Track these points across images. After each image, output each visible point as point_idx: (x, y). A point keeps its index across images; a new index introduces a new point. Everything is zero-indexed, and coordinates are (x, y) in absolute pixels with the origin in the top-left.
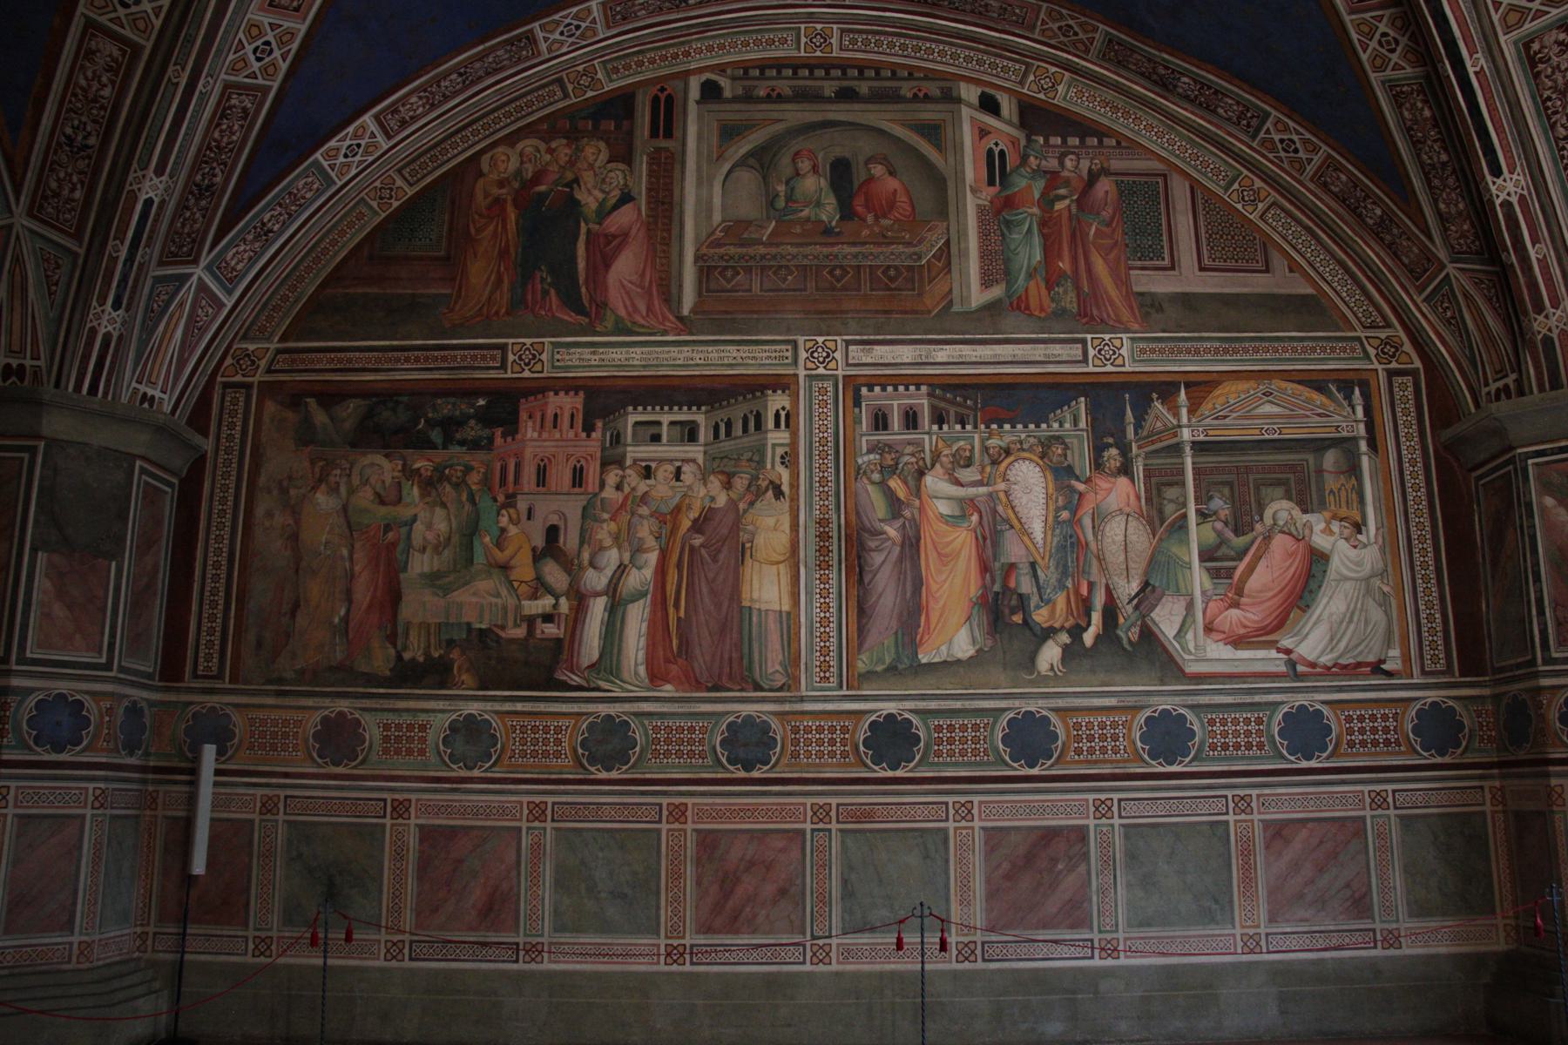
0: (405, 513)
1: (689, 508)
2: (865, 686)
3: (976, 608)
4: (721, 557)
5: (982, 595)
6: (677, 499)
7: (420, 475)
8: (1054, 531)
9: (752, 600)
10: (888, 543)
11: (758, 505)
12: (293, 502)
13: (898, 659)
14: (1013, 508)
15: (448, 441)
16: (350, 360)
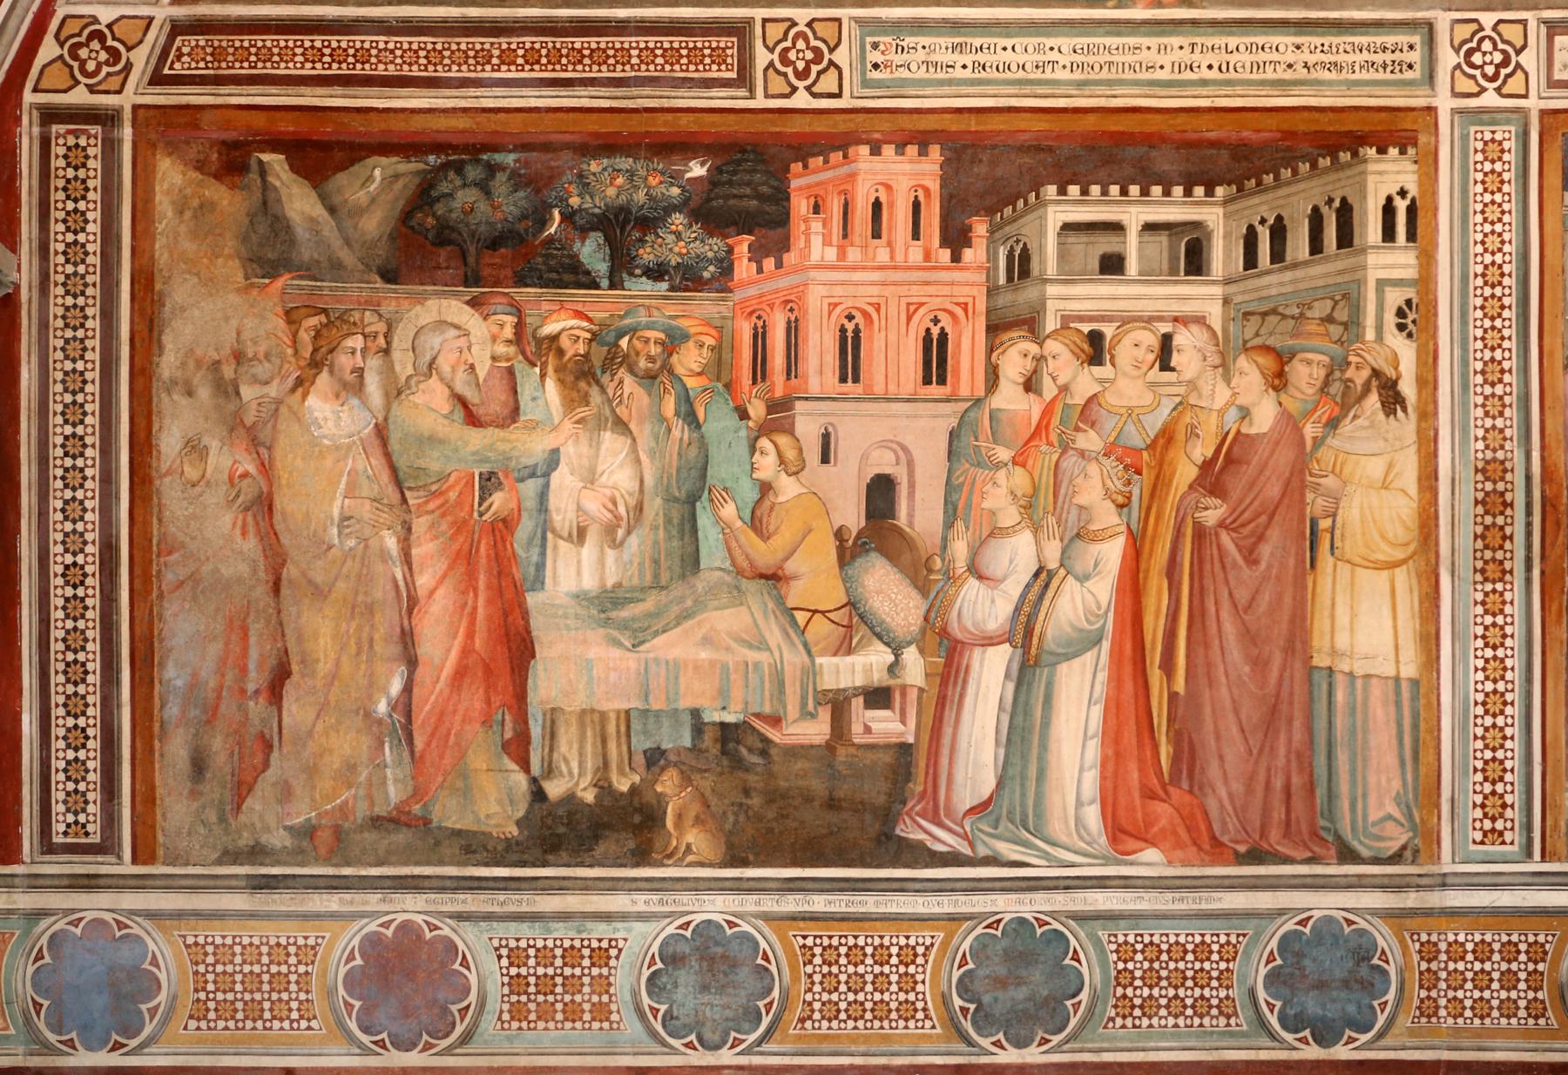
0: (534, 447)
1: (1192, 433)
4: (1265, 550)
6: (1164, 412)
7: (561, 352)
9: (1334, 652)
11: (1346, 427)
12: (249, 419)
15: (622, 264)
16: (362, 56)
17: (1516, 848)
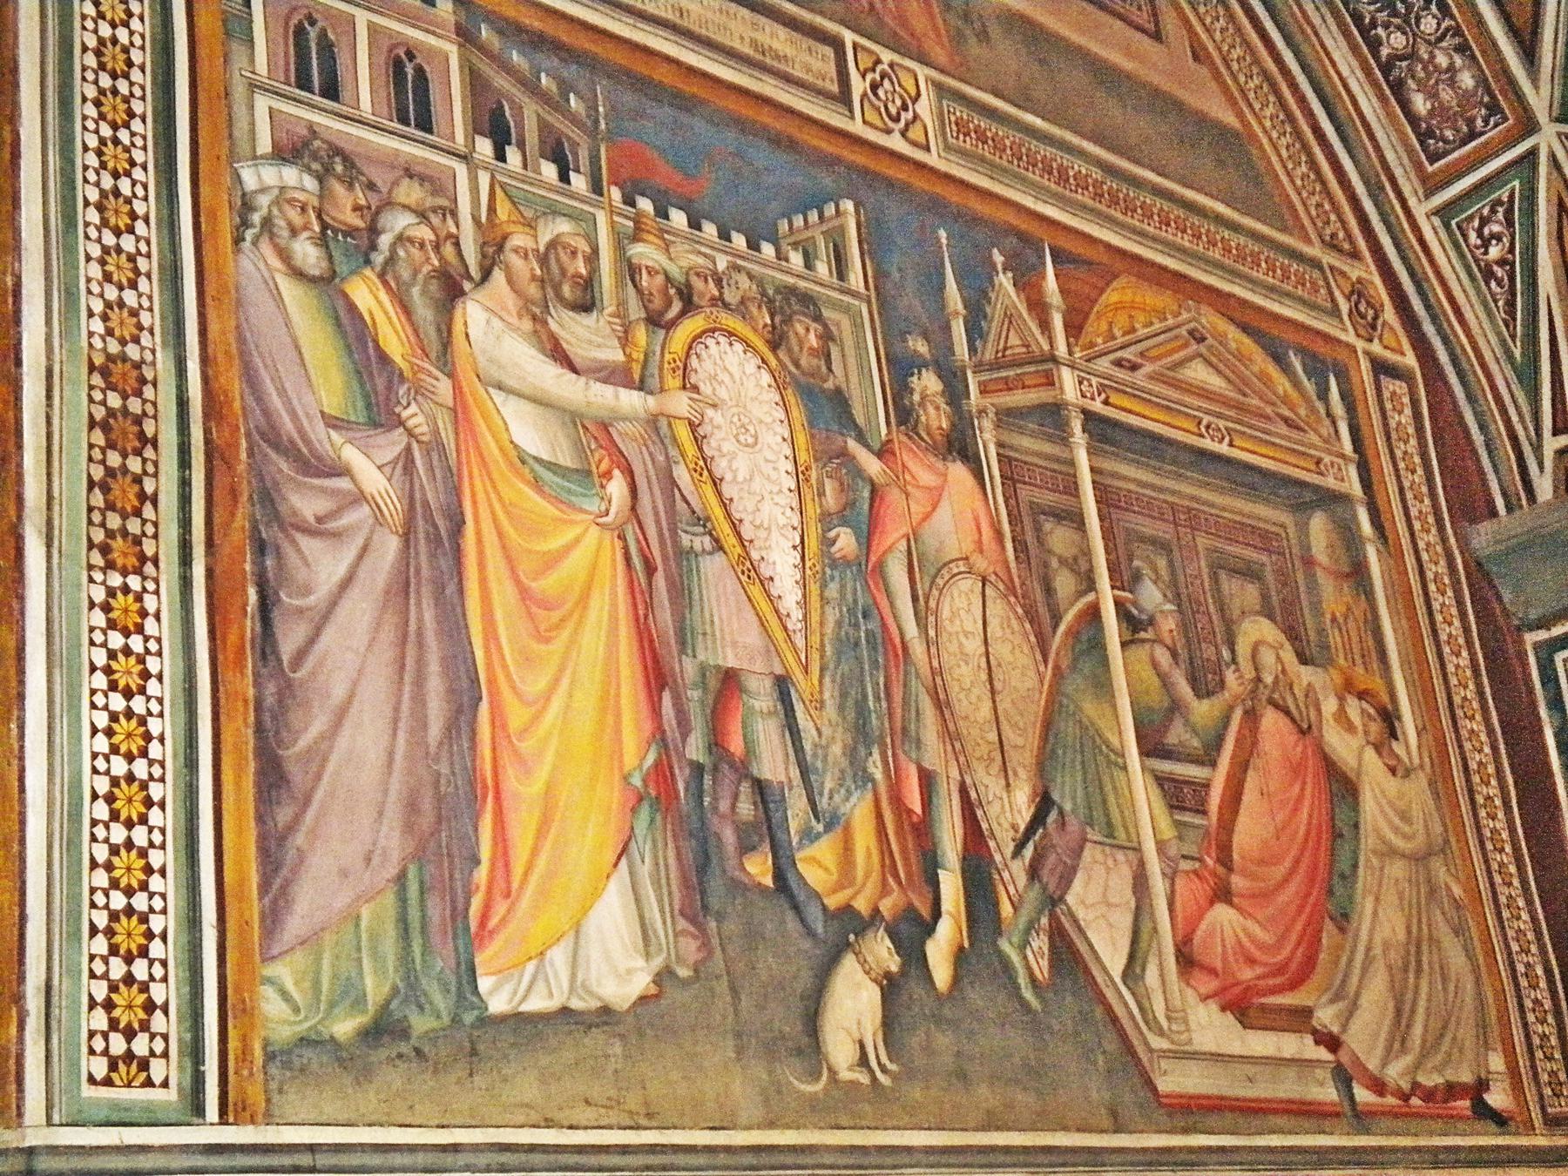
2: (293, 1101)
3: (645, 812)
5: (657, 765)
8: (824, 586)
10: (365, 510)
13: (410, 989)
14: (716, 483)
17: (171, 1095)
